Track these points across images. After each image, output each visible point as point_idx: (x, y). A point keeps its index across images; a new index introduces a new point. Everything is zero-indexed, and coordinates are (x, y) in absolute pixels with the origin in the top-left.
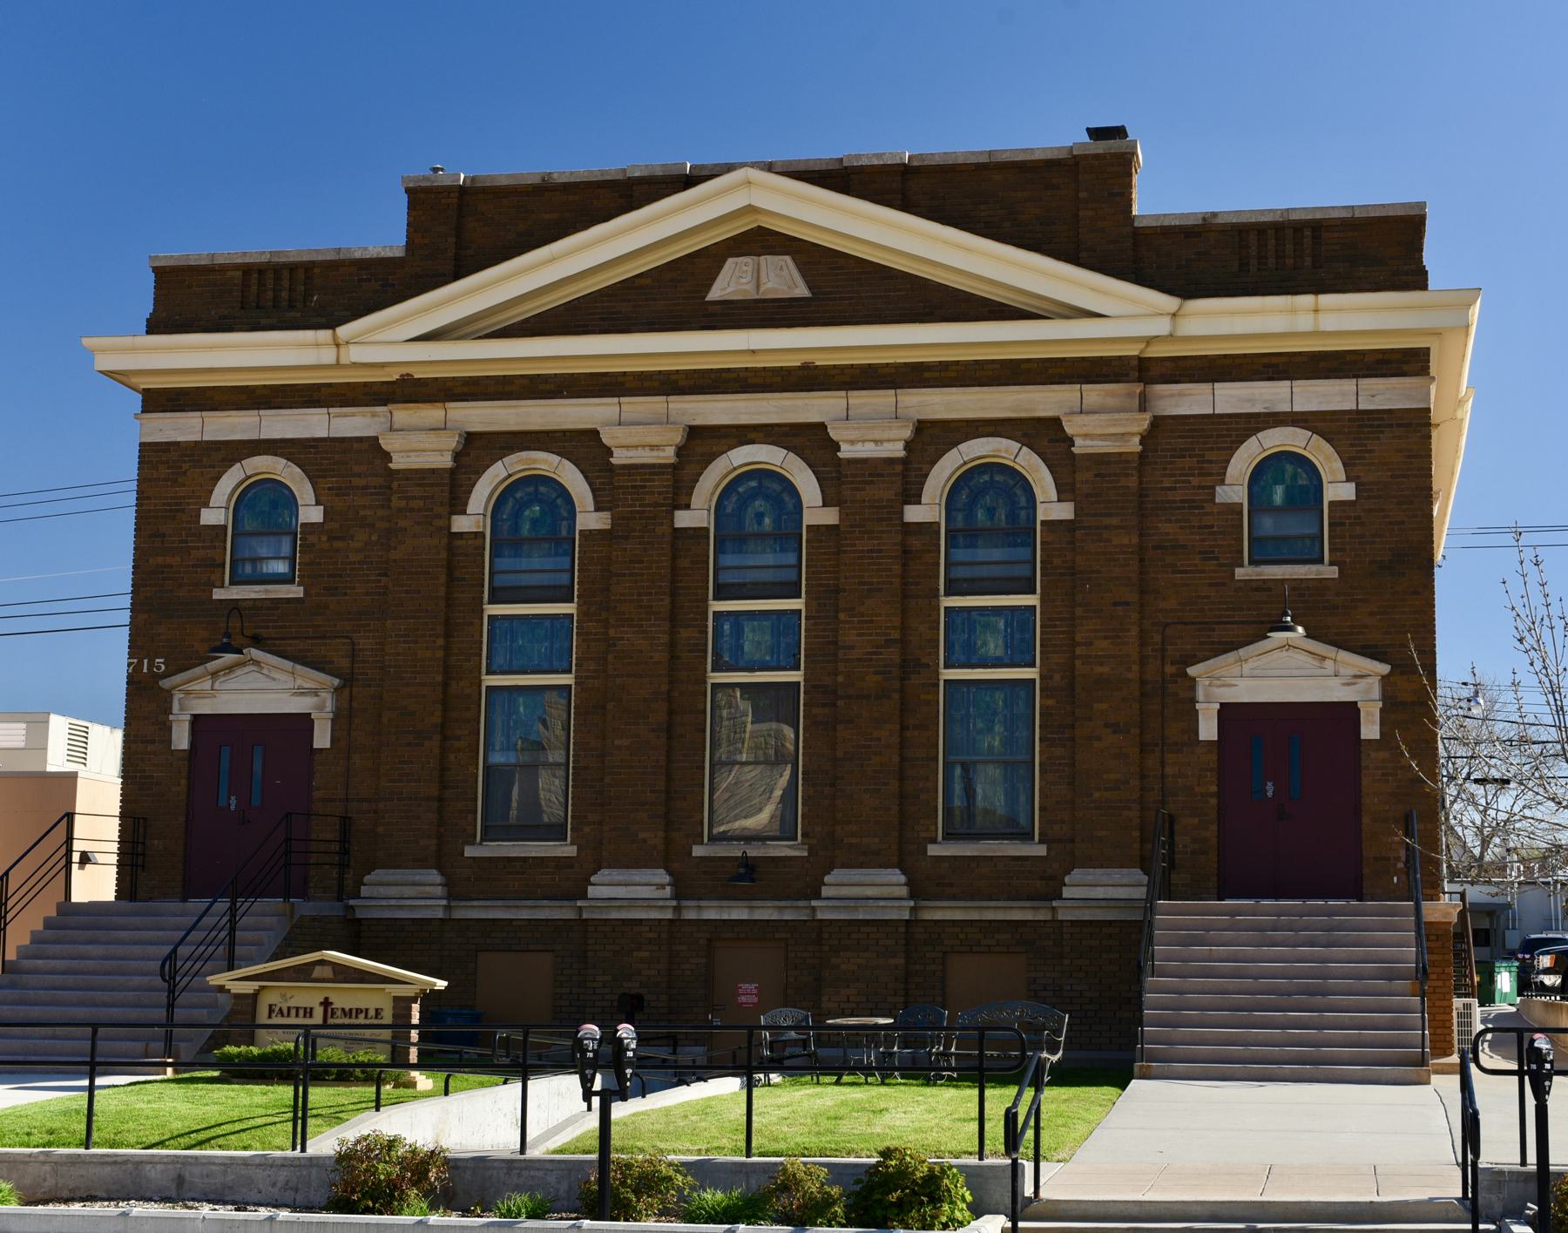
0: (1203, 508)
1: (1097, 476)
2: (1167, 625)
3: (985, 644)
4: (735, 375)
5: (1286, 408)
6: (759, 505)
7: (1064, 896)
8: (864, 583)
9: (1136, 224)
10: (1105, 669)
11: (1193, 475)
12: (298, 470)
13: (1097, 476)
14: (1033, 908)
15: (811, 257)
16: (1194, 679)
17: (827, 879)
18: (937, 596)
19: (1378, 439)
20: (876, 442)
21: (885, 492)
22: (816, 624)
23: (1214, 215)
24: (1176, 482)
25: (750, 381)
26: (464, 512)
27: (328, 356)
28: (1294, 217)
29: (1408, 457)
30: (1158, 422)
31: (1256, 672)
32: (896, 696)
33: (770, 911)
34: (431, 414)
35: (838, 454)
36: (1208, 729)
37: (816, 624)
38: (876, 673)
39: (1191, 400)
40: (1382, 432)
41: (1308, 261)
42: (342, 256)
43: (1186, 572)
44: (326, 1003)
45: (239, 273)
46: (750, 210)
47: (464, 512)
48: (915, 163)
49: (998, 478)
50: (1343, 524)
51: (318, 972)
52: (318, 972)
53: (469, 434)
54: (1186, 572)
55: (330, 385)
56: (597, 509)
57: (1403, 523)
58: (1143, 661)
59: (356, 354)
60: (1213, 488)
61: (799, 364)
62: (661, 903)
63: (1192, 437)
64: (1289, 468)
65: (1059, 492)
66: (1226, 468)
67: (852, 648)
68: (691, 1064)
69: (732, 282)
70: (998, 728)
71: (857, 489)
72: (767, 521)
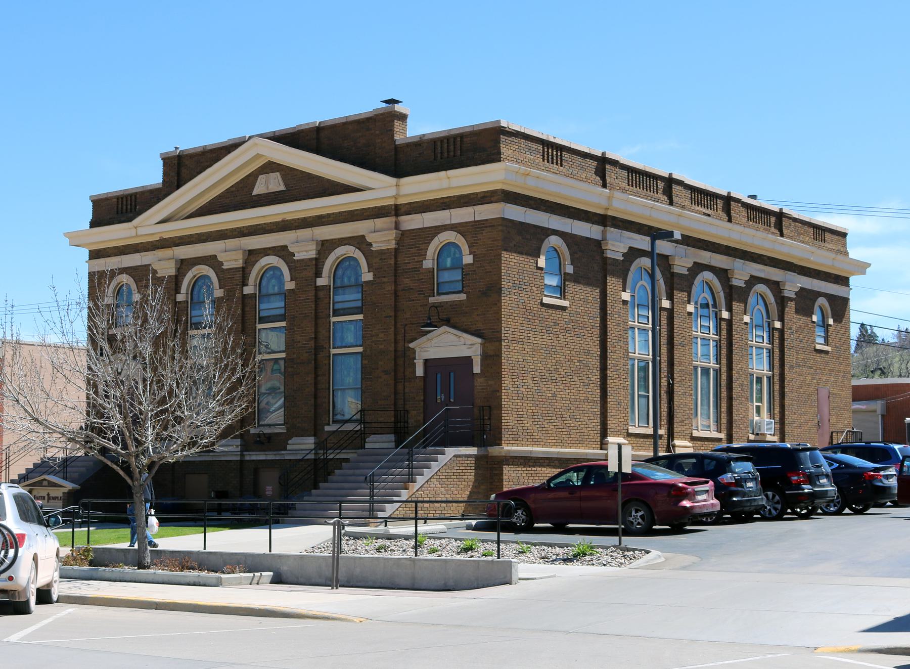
0: (419, 271)
1: (380, 259)
2: (406, 325)
3: (347, 337)
4: (261, 227)
5: (448, 222)
6: (273, 281)
7: (366, 447)
8: (302, 314)
9: (397, 143)
10: (382, 347)
11: (416, 256)
12: (132, 279)
13: (380, 259)
14: (275, 454)
15: (288, 173)
16: (413, 349)
17: (290, 442)
18: (330, 317)
19: (482, 233)
20: (306, 251)
21: (310, 272)
22: (289, 332)
23: (424, 135)
24: (410, 260)
25: (267, 228)
26: (180, 293)
27: (133, 232)
28: (453, 133)
29: (493, 241)
30: (404, 233)
31: (437, 345)
32: (313, 362)
33: (271, 456)
34: (168, 252)
35: (223, 267)
36: (420, 372)
37: (289, 332)
38: (306, 352)
39: (412, 222)
40: (484, 230)
41: (459, 153)
42: (144, 189)
43: (413, 300)
44: (48, 495)
45: (115, 200)
46: (258, 156)
47: (180, 293)
48: (322, 125)
49: (352, 263)
50: (469, 274)
51: (45, 483)
52: (45, 483)
53: (182, 260)
54: (413, 300)
55: (141, 243)
56: (220, 288)
57: (490, 272)
58: (396, 342)
59: (141, 231)
60: (422, 261)
61: (281, 220)
62: (235, 453)
63: (416, 239)
64: (453, 249)
65: (369, 268)
66: (426, 252)
67: (299, 342)
68: (427, 521)
69: (260, 188)
70: (352, 374)
71: (300, 273)
72: (276, 288)
